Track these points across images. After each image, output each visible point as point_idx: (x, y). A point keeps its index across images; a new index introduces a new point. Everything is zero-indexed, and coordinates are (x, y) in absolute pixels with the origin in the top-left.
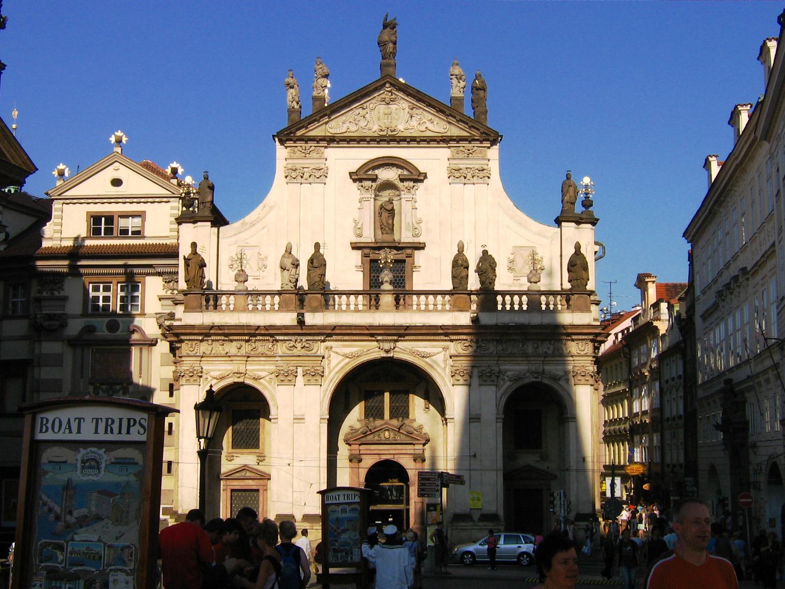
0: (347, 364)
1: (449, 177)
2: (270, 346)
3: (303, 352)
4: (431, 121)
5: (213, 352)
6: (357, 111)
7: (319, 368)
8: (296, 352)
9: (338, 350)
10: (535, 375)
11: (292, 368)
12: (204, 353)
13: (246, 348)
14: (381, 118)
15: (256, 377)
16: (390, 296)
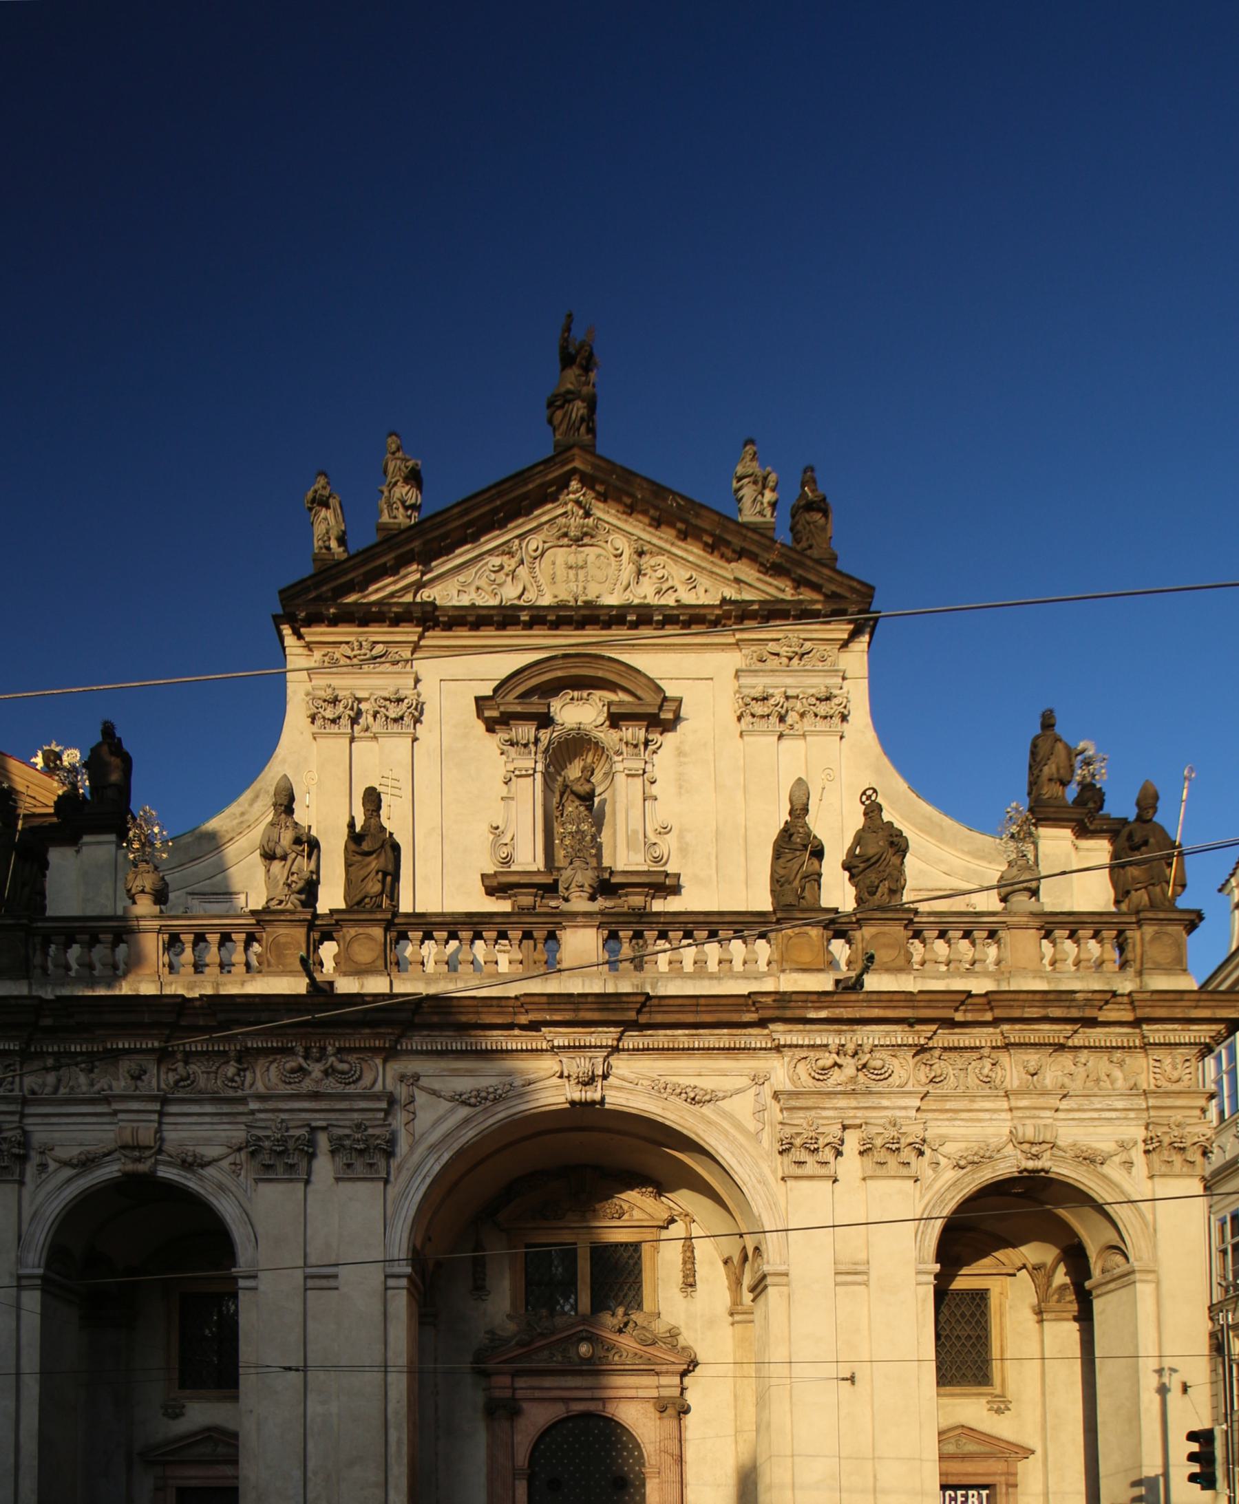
0: (466, 1121)
1: (739, 719)
2: (231, 1070)
3: (331, 1086)
4: (691, 583)
5: (62, 1090)
6: (496, 561)
7: (377, 1131)
8: (307, 1085)
9: (436, 1085)
10: (1034, 1150)
11: (297, 1132)
12: (33, 1092)
13: (157, 1079)
14: (558, 579)
15: (190, 1159)
16: (592, 932)
